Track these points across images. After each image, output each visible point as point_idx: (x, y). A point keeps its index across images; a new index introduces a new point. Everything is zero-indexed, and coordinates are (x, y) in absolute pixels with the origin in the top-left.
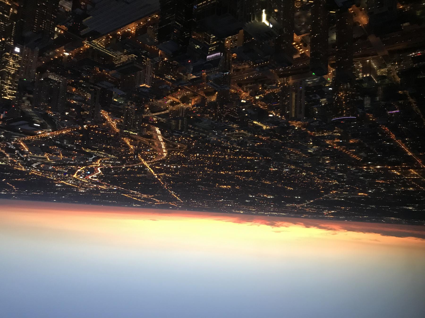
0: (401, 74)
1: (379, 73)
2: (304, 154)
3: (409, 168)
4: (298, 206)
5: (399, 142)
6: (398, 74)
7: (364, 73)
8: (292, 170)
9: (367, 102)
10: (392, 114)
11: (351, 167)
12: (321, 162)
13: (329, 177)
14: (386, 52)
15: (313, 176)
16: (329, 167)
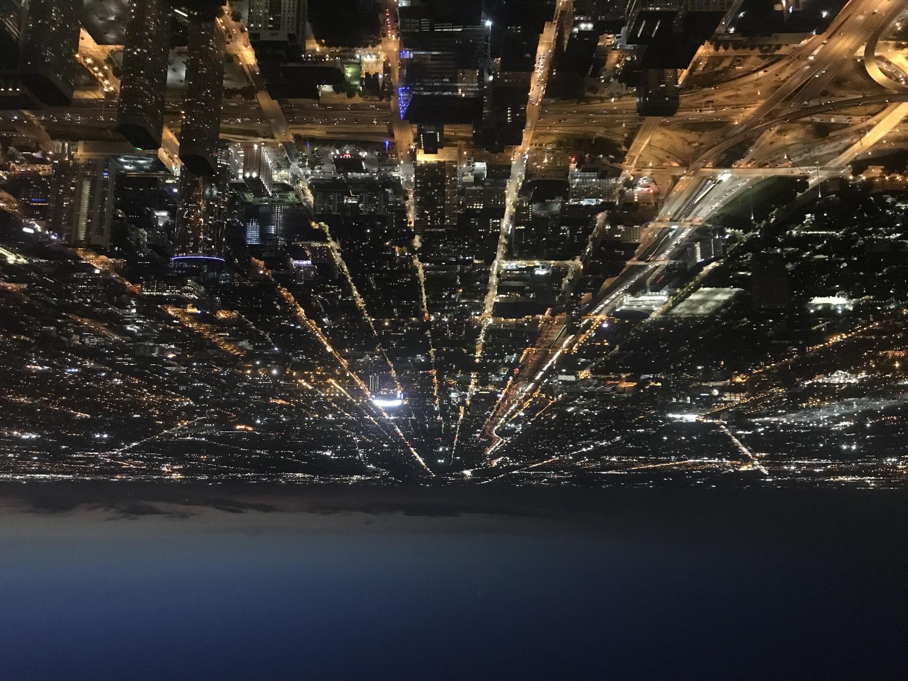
0: (317, 187)
1: (276, 178)
2: (119, 335)
3: (329, 377)
4: (101, 456)
5: (312, 324)
6: (310, 187)
7: (246, 169)
8: (86, 374)
9: (253, 235)
10: (299, 267)
11: (221, 369)
12: (155, 355)
13: (176, 390)
14: (291, 138)
15: (139, 386)
16: (174, 369)
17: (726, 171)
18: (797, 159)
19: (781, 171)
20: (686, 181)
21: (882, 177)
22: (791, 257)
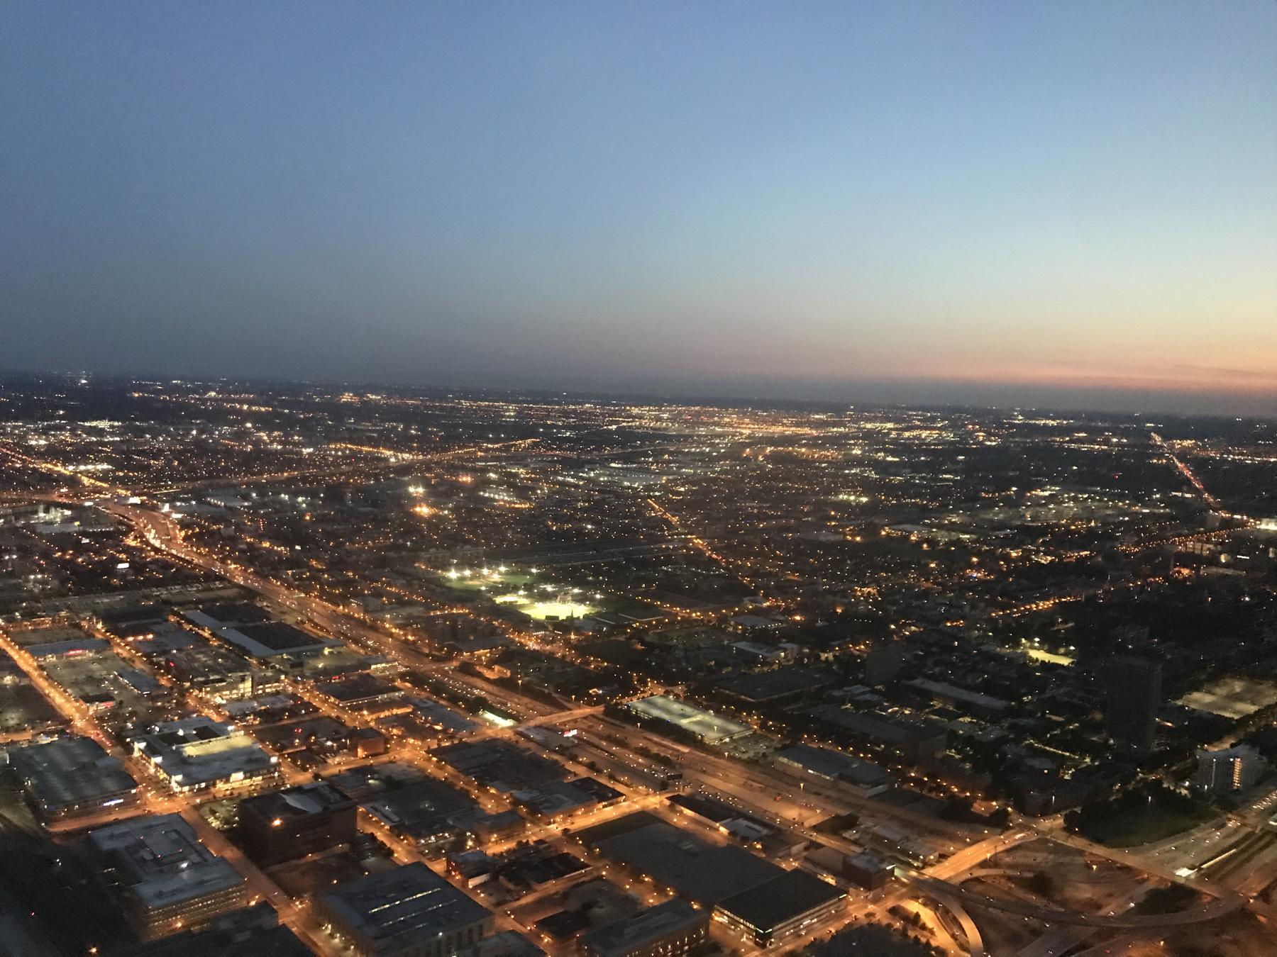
17: (1182, 881)
18: (1079, 860)
19: (1100, 851)
20: (1250, 886)
21: (974, 798)
22: (1096, 728)
